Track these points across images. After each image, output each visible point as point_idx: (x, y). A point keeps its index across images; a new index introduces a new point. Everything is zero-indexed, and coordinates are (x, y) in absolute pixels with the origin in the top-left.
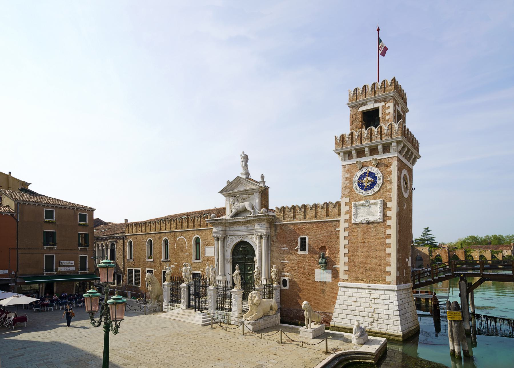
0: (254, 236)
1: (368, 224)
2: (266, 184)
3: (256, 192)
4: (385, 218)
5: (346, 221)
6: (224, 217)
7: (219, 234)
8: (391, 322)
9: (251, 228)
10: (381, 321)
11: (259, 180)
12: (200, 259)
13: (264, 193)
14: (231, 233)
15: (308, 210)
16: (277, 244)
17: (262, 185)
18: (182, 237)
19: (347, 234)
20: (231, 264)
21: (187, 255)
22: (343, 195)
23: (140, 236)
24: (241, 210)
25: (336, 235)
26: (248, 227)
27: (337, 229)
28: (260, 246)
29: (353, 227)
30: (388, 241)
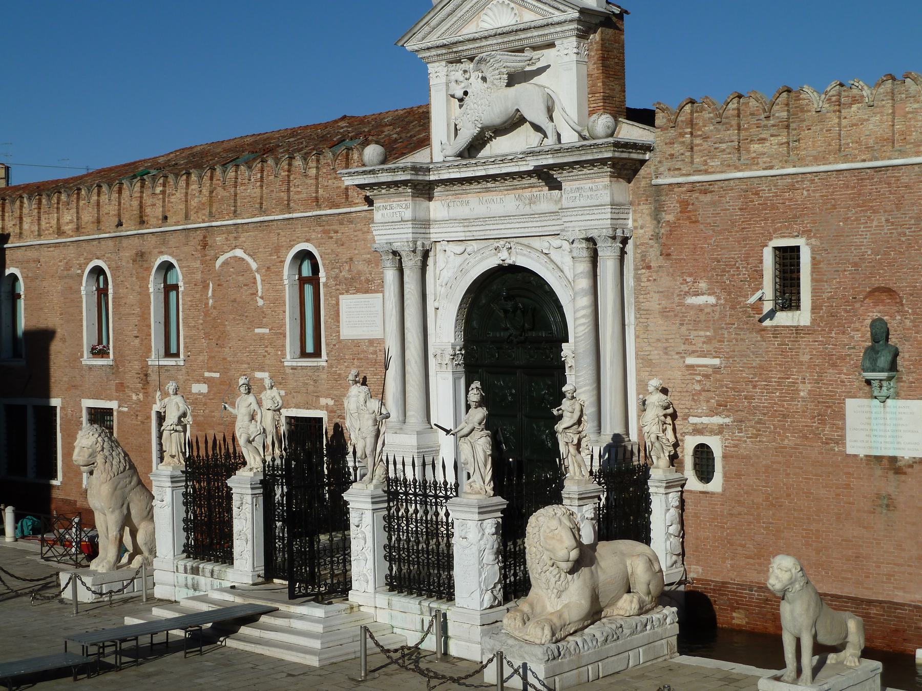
7: (402, 237)
12: (317, 353)
16: (665, 281)
18: (239, 253)
20: (461, 369)
21: (262, 337)
23: (56, 252)
26: (531, 201)
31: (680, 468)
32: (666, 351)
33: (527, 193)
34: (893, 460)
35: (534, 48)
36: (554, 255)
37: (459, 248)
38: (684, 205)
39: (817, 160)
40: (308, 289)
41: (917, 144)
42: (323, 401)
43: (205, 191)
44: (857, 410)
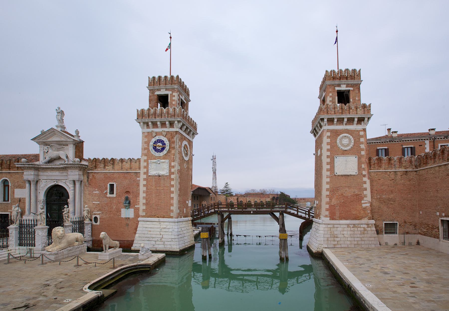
0: (67, 181)
1: (160, 176)
2: (80, 138)
3: (70, 144)
4: (171, 173)
5: (144, 173)
6: (37, 163)
8: (172, 243)
9: (65, 174)
10: (166, 243)
11: (74, 134)
12: (8, 201)
14: (45, 178)
15: (116, 163)
16: (89, 189)
17: (76, 139)
19: (145, 183)
22: (143, 154)
24: (55, 158)
25: (137, 183)
26: (62, 173)
27: (138, 179)
28: (75, 190)
29: (149, 178)
30: (172, 189)
31: (91, 220)
32: (89, 201)
33: (61, 171)
34: (129, 218)
35: (64, 145)
36: (67, 183)
37: (45, 181)
38: (93, 176)
39: (117, 170)
40: (7, 188)
41: (134, 169)
42: (9, 210)
44: (123, 210)
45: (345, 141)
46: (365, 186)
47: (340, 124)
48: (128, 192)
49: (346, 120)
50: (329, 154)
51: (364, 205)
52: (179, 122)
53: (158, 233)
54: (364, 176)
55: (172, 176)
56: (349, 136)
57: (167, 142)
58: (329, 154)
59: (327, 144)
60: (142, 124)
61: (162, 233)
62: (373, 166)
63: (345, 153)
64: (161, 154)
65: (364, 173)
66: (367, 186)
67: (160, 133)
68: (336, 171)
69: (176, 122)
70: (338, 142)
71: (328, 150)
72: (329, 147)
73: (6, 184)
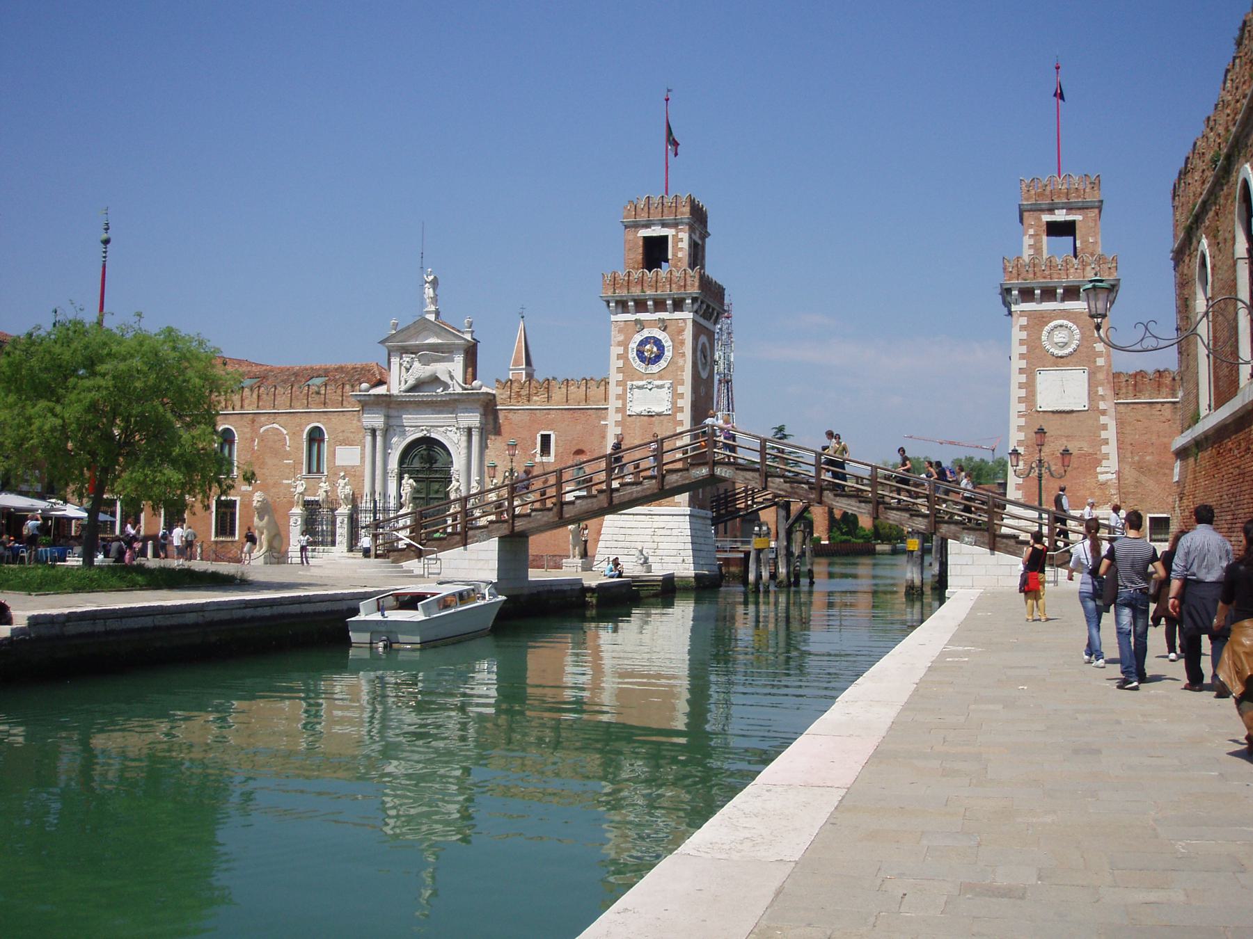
3: (458, 349)
5: (618, 410)
13: (471, 354)
17: (468, 337)
18: (275, 426)
29: (627, 419)
43: (255, 396)
45: (1059, 337)
46: (1104, 434)
47: (1049, 300)
48: (579, 452)
49: (1060, 291)
50: (1023, 364)
51: (1102, 478)
52: (694, 300)
53: (648, 538)
54: (1104, 412)
55: (679, 416)
56: (1070, 324)
57: (667, 343)
58: (1023, 364)
59: (1021, 344)
60: (612, 304)
61: (656, 539)
62: (1124, 391)
63: (1059, 361)
64: (655, 369)
65: (1102, 406)
66: (1111, 434)
67: (652, 324)
68: (1039, 403)
69: (688, 301)
70: (1044, 338)
71: (1022, 356)
72: (1024, 349)
73: (317, 435)
